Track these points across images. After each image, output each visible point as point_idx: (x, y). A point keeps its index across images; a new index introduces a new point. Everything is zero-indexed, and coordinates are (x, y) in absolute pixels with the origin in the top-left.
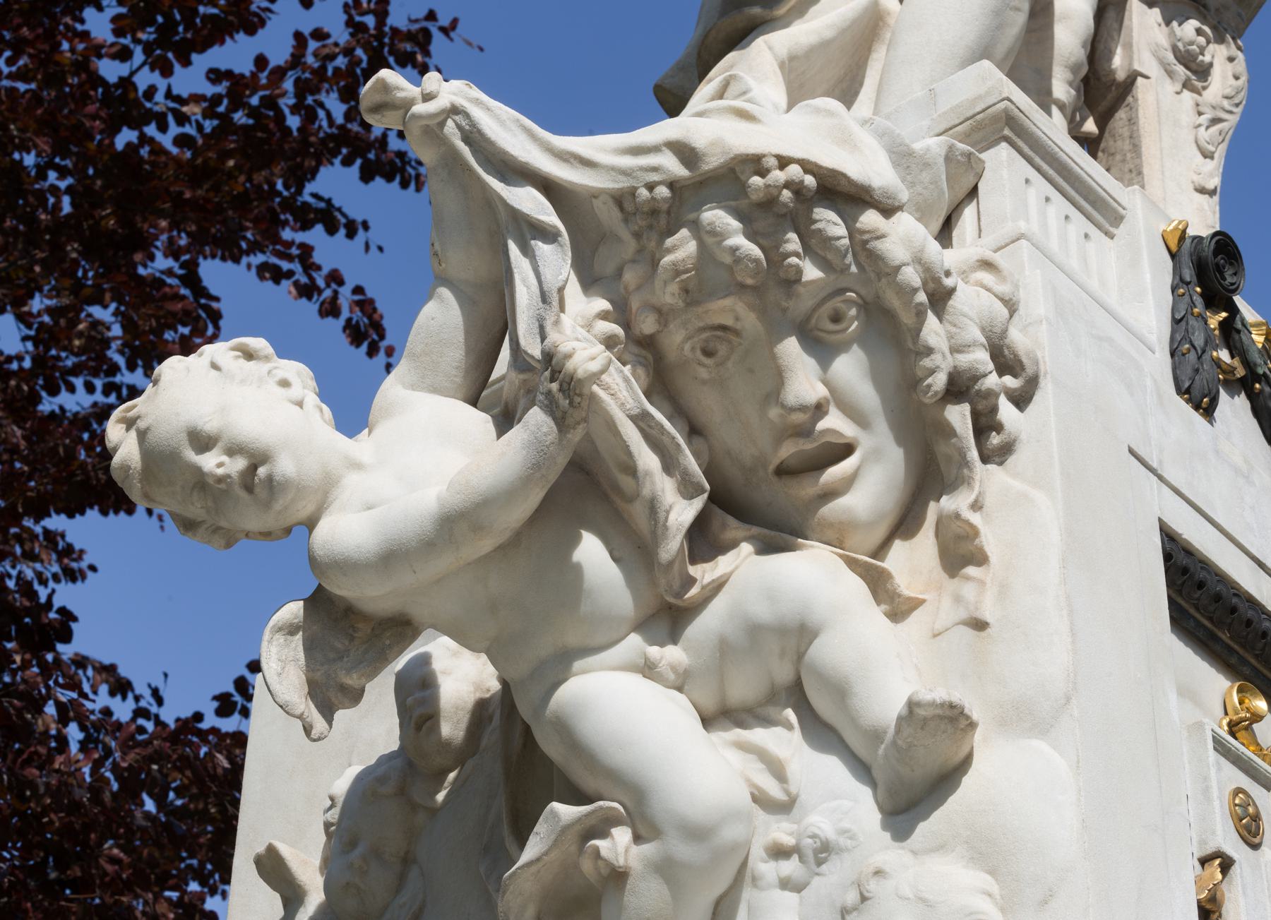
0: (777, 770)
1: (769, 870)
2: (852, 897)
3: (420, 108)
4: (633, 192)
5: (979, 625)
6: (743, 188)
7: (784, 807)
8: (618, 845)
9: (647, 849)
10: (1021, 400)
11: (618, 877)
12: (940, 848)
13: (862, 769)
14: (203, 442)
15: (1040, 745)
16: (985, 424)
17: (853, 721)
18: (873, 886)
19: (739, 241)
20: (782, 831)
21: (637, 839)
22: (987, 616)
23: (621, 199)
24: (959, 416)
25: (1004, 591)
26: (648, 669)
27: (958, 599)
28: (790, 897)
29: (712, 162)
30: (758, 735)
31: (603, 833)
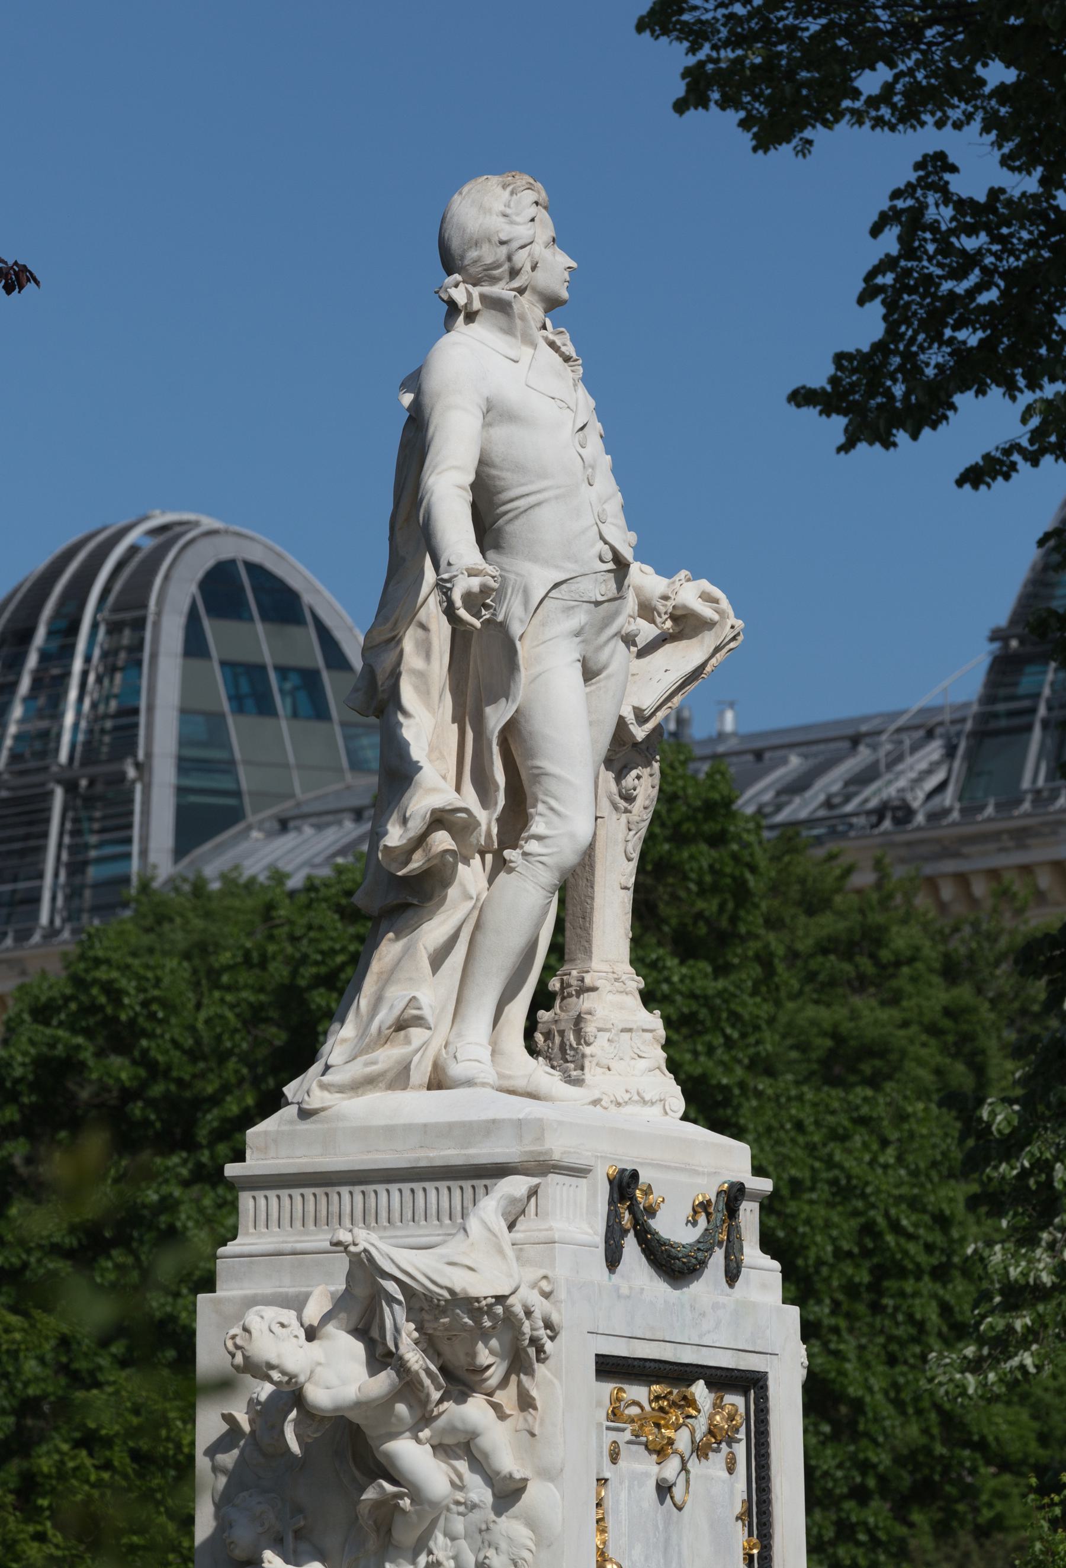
0: (460, 1476)
2: (484, 1527)
5: (533, 1435)
6: (471, 1304)
8: (406, 1503)
12: (516, 1517)
14: (271, 1367)
15: (551, 1485)
16: (540, 1350)
17: (489, 1466)
18: (491, 1525)
19: (466, 1320)
24: (532, 1351)
25: (542, 1424)
26: (418, 1441)
27: (526, 1420)
28: (461, 1518)
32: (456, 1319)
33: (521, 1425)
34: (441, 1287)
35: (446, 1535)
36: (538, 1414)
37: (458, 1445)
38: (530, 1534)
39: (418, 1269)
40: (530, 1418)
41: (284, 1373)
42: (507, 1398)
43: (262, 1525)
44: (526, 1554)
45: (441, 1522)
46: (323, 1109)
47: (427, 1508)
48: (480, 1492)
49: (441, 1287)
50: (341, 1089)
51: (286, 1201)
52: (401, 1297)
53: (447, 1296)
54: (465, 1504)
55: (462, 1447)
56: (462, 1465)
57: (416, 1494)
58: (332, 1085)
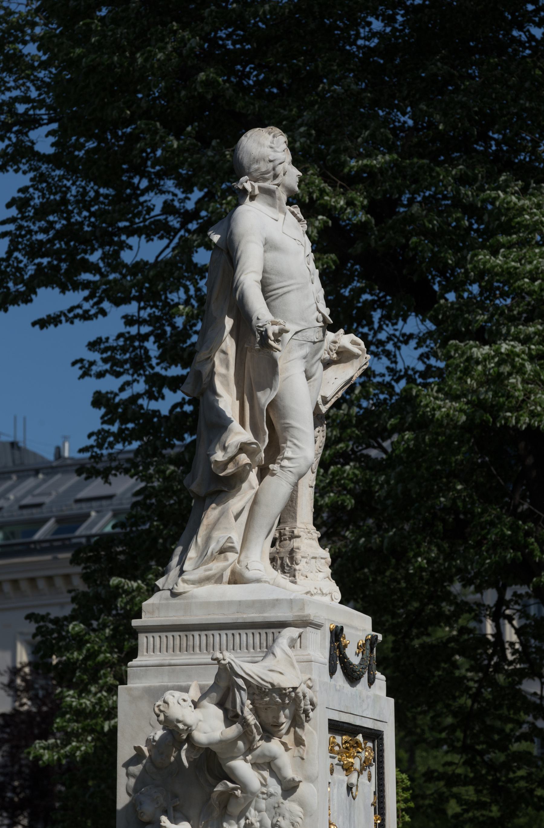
0: (265, 779)
1: (260, 795)
3: (223, 662)
5: (303, 759)
8: (238, 793)
10: (312, 710)
11: (237, 797)
12: (293, 801)
14: (179, 721)
16: (307, 716)
17: (281, 774)
20: (264, 790)
21: (242, 792)
26: (246, 761)
30: (262, 772)
32: (273, 698)
33: (296, 754)
35: (255, 809)
36: (305, 749)
37: (264, 763)
38: (301, 809)
40: (301, 750)
41: (185, 725)
42: (289, 739)
44: (299, 820)
45: (253, 803)
46: (184, 593)
47: (249, 795)
48: (275, 787)
50: (193, 582)
51: (164, 639)
52: (245, 687)
55: (268, 764)
56: (266, 774)
57: (244, 788)
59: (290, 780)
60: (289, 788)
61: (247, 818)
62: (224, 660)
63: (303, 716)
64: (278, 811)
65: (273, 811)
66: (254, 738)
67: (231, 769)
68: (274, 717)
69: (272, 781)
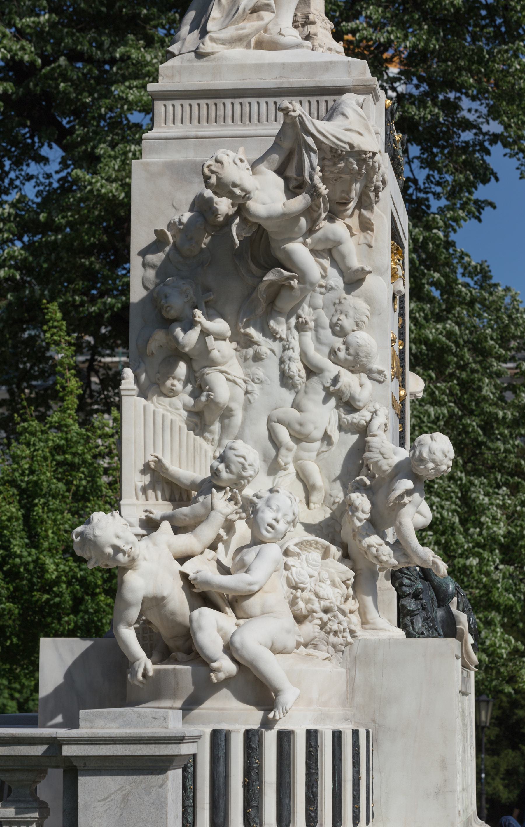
0: (324, 269)
1: (318, 289)
2: (337, 301)
3: (292, 113)
4: (337, 150)
5: (370, 246)
6: (360, 155)
7: (323, 277)
8: (295, 283)
9: (301, 286)
11: (292, 288)
12: (358, 296)
13: (342, 273)
14: (235, 185)
15: (380, 278)
18: (343, 301)
19: (355, 166)
20: (323, 282)
21: (299, 282)
22: (373, 244)
23: (331, 148)
26: (305, 244)
27: (365, 238)
28: (321, 296)
29: (356, 149)
30: (321, 260)
31: (293, 280)
32: (348, 164)
33: (362, 240)
34: (345, 142)
35: (310, 306)
36: (374, 234)
37: (323, 250)
38: (368, 307)
39: (327, 132)
40: (368, 237)
41: (243, 190)
42: (354, 222)
43: (187, 296)
44: (365, 319)
45: (308, 299)
46: (213, 53)
47: (308, 286)
48: (336, 279)
49: (345, 142)
50: (223, 42)
51: (187, 108)
52: (316, 148)
53: (348, 149)
54: (326, 287)
55: (330, 251)
56: (326, 263)
57: (303, 277)
58: (218, 39)
59: (357, 271)
60: (354, 281)
61: (299, 317)
62: (294, 111)
63: (372, 195)
64: (339, 307)
65: (333, 309)
66: (320, 215)
67: (288, 255)
68: (343, 191)
69: (333, 272)
